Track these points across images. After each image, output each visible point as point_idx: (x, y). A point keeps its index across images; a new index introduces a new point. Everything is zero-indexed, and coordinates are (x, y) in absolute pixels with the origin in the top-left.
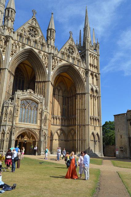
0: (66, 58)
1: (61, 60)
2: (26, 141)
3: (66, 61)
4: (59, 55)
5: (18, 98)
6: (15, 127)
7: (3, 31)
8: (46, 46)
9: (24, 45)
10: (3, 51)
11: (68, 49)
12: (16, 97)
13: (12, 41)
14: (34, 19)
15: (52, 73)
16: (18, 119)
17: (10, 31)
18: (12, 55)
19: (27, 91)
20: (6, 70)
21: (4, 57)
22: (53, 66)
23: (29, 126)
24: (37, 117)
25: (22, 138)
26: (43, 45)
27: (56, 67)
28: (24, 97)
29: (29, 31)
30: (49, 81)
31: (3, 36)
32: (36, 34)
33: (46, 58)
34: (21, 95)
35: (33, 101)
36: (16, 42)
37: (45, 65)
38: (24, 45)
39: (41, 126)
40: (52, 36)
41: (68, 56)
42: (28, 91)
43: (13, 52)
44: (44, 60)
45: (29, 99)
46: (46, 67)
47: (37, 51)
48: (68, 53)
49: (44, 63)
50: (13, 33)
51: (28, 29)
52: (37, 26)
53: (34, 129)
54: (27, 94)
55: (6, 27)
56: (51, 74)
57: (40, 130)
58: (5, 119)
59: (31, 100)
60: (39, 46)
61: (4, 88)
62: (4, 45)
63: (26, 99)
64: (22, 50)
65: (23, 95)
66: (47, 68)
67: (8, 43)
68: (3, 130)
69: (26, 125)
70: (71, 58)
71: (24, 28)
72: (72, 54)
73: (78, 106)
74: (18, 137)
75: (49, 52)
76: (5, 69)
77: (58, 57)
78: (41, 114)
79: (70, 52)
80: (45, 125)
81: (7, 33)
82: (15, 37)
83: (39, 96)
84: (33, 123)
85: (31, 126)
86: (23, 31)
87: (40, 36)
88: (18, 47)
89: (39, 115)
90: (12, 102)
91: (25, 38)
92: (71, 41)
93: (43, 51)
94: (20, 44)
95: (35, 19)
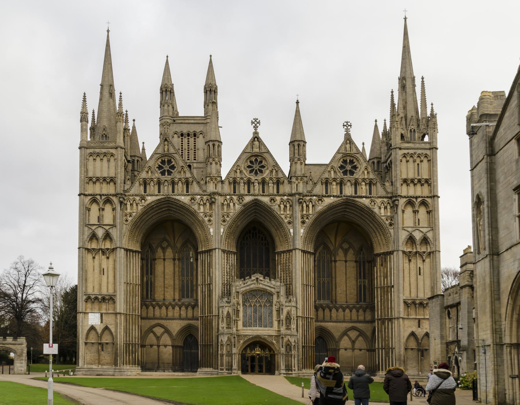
0: (335, 189)
1: (320, 198)
2: (258, 354)
3: (334, 196)
4: (319, 189)
5: (238, 292)
6: (236, 336)
7: (204, 188)
8: (286, 181)
9: (241, 197)
10: (209, 221)
11: (341, 167)
12: (234, 291)
13: (220, 200)
14: (256, 139)
15: (302, 231)
16: (240, 323)
17: (216, 182)
18: (224, 221)
19: (250, 278)
20: (217, 250)
21: (211, 230)
22: (302, 218)
23: (260, 332)
24: (272, 317)
25: (251, 351)
26: (278, 183)
27: (311, 216)
28: (248, 288)
29: (249, 167)
30: (295, 249)
31: (205, 195)
32: (263, 167)
33: (288, 205)
34: (243, 285)
35: (264, 291)
36: (228, 197)
37: (286, 221)
38: (241, 197)
39: (280, 331)
40: (296, 155)
41: (341, 184)
42: (253, 278)
43: (225, 217)
44: (282, 213)
45: (256, 290)
46: (289, 223)
47: (266, 200)
48: (340, 175)
49: (283, 216)
50: (220, 183)
51: (246, 164)
52: (263, 150)
53: (269, 336)
54: (252, 282)
55: (208, 179)
56: (298, 233)
57: (279, 336)
58: (223, 326)
59: (259, 290)
60: (271, 188)
61: (217, 279)
62: (208, 211)
63: (251, 291)
64: (240, 206)
65: (246, 285)
66: (289, 226)
67: (213, 206)
68: (222, 340)
69: (255, 332)
70: (349, 184)
71: (238, 166)
72: (352, 173)
73: (379, 281)
74: (245, 349)
75: (293, 192)
76: (215, 249)
77: (314, 196)
78: (279, 311)
79: (345, 173)
80: (288, 328)
81: (211, 188)
82: (227, 189)
83: (273, 282)
84: (266, 326)
85: (264, 332)
86: (238, 171)
87: (270, 169)
88: (231, 204)
89: (275, 313)
90: (228, 299)
91: (242, 184)
92: (348, 146)
93: (280, 195)
94: (235, 198)
95: (258, 139)
